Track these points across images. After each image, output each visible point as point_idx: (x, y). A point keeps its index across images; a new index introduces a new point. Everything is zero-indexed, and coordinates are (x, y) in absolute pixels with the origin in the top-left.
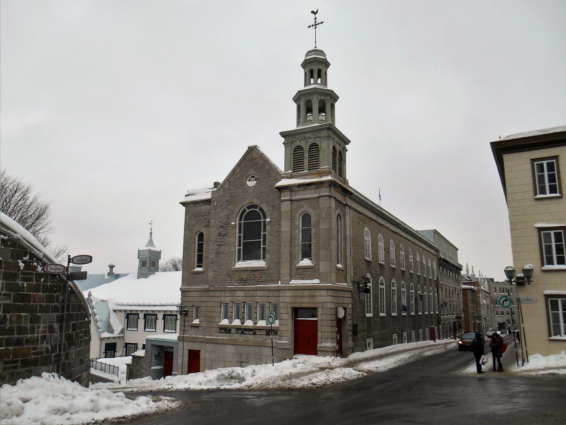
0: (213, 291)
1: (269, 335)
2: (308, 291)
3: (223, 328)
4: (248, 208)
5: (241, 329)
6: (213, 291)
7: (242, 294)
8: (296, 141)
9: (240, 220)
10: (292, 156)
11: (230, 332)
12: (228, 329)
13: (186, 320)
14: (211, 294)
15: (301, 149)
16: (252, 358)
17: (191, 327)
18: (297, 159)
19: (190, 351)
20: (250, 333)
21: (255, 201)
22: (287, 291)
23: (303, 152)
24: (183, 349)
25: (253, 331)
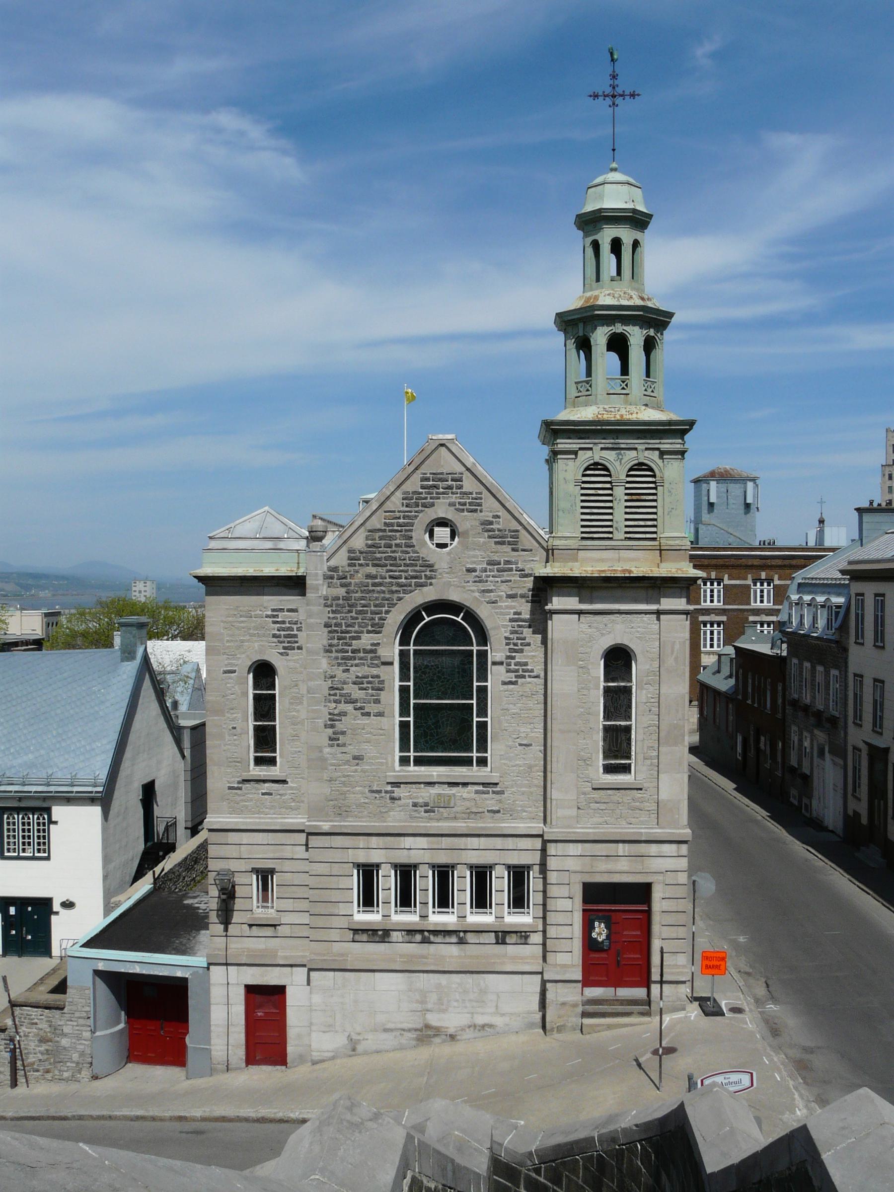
1: (504, 943)
2: (626, 845)
3: (364, 931)
5: (421, 932)
7: (422, 842)
8: (591, 449)
9: (404, 641)
11: (386, 940)
15: (602, 472)
16: (457, 1001)
17: (251, 926)
20: (448, 940)
22: (571, 845)
24: (228, 984)
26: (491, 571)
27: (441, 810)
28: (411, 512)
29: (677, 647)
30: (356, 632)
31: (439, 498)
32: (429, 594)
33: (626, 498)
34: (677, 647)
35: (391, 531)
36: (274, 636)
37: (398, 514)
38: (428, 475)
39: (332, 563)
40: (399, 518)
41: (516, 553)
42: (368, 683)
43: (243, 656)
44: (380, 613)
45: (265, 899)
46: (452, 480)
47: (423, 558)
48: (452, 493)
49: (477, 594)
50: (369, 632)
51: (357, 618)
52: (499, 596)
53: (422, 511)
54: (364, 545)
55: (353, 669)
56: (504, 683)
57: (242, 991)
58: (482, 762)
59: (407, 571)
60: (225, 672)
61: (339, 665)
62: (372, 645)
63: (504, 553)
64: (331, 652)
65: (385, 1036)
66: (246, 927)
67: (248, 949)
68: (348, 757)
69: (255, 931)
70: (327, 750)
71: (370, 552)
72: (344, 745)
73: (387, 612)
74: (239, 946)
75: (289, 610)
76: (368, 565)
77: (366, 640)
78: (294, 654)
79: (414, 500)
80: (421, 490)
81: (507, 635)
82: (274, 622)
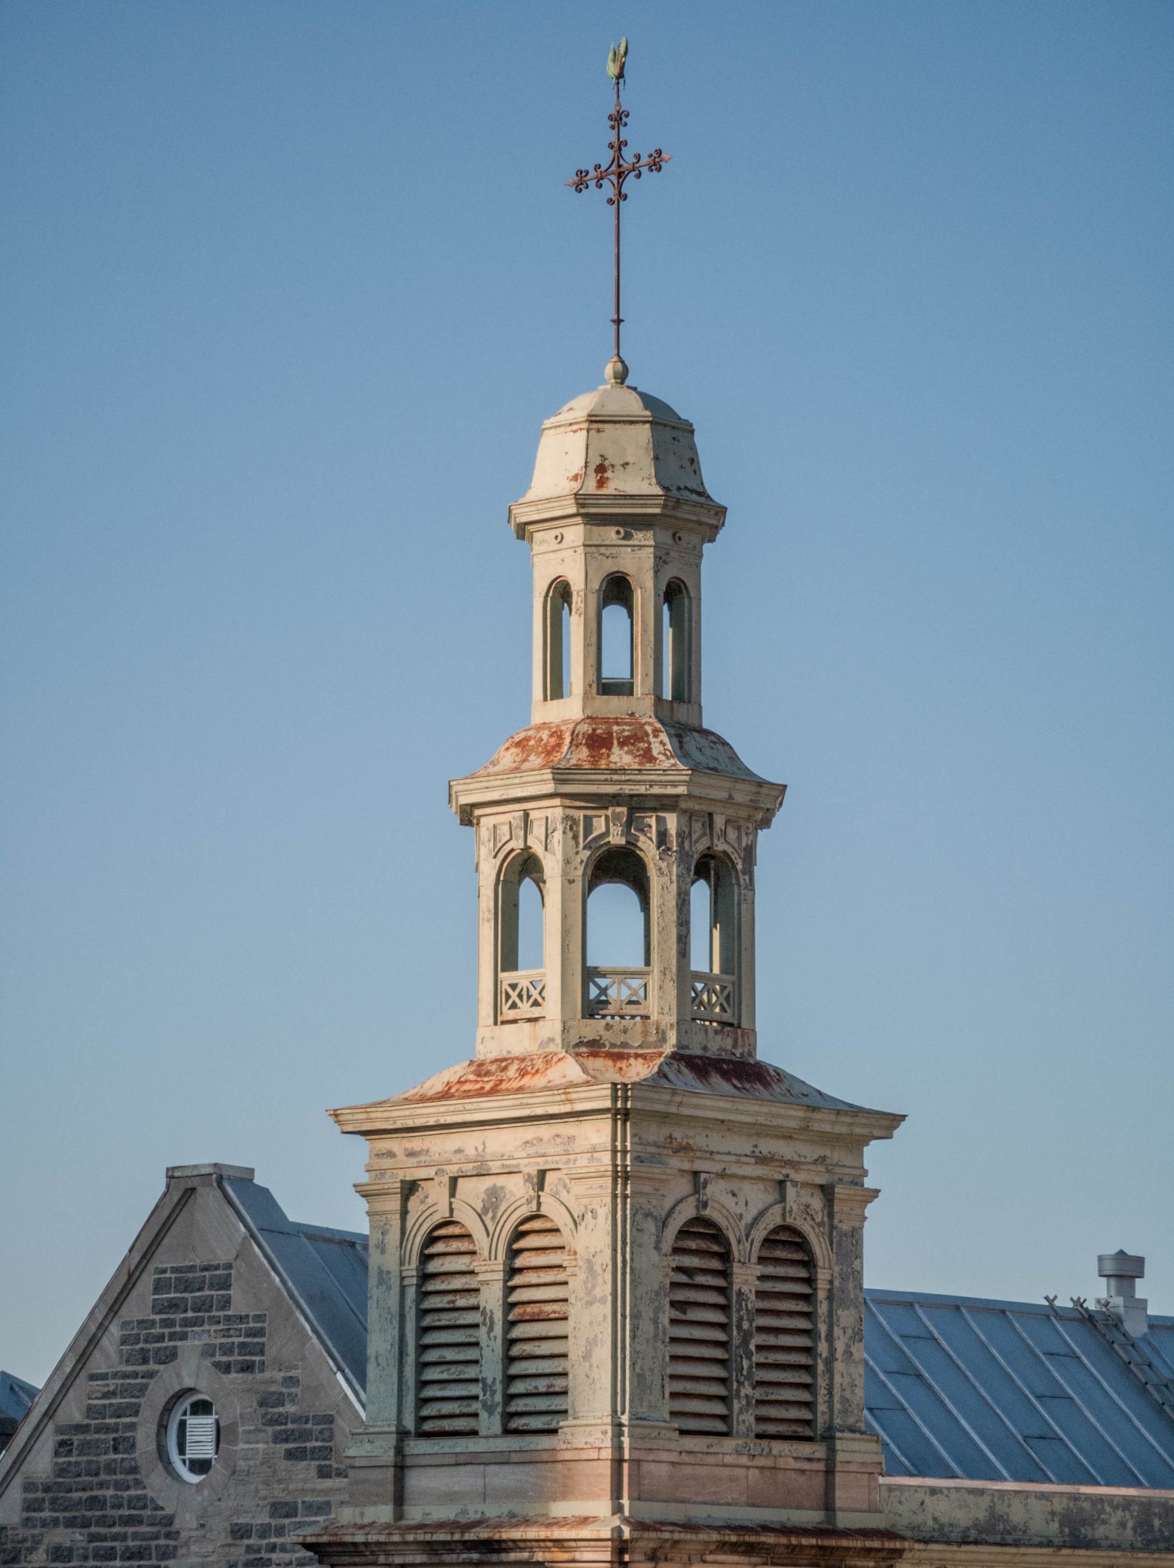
28: (135, 1375)
31: (183, 1337)
35: (99, 1430)
37: (112, 1384)
38: (168, 1275)
40: (113, 1394)
41: (327, 1483)
47: (152, 1500)
53: (151, 1375)
54: (49, 1467)
59: (124, 1537)
76: (55, 1522)
79: (141, 1345)
80: (152, 1317)
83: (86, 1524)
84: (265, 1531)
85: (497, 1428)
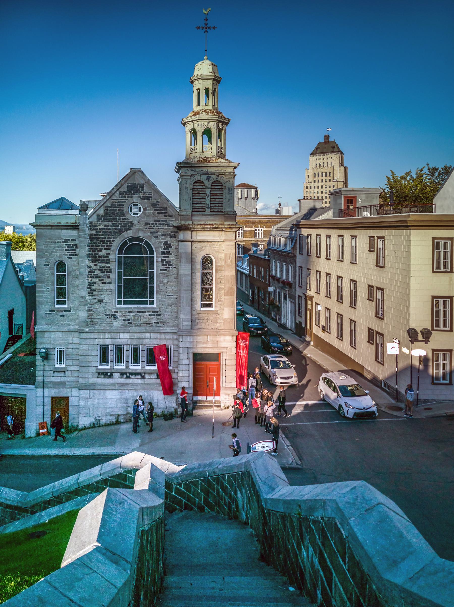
0: (87, 332)
3: (103, 373)
4: (130, 240)
5: (126, 374)
6: (87, 332)
7: (127, 336)
10: (191, 191)
12: (109, 374)
13: (46, 363)
14: (84, 336)
17: (54, 372)
18: (197, 195)
19: (54, 400)
20: (137, 377)
21: (141, 234)
23: (204, 188)
25: (141, 375)
26: (156, 224)
27: (135, 323)
29: (231, 256)
30: (100, 249)
31: (134, 194)
32: (130, 234)
33: (211, 195)
34: (231, 256)
35: (114, 207)
36: (66, 250)
37: (117, 201)
39: (90, 220)
42: (105, 270)
43: (53, 258)
44: (110, 241)
45: (61, 360)
46: (140, 187)
48: (140, 192)
49: (149, 234)
50: (105, 249)
51: (100, 243)
52: (158, 235)
53: (127, 200)
55: (99, 264)
56: (161, 270)
57: (50, 399)
58: (152, 303)
60: (45, 265)
61: (93, 262)
62: (107, 254)
63: (161, 217)
64: (90, 257)
65: (111, 418)
66: (52, 372)
67: (53, 382)
68: (96, 301)
69: (56, 374)
70: (88, 298)
71: (106, 216)
72: (95, 295)
73: (113, 241)
74: (49, 380)
75: (72, 240)
76: (105, 221)
77: (104, 252)
78: (74, 258)
81: (163, 250)
82: (66, 245)
83: (112, 222)
84: (152, 224)
85: (209, 210)
